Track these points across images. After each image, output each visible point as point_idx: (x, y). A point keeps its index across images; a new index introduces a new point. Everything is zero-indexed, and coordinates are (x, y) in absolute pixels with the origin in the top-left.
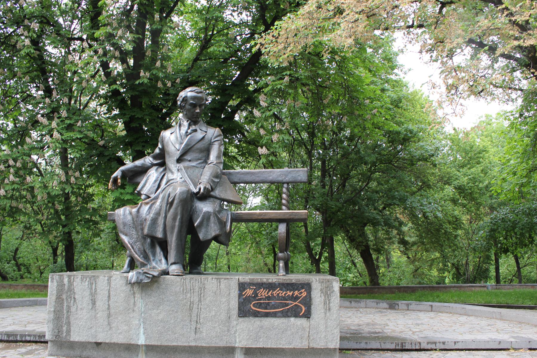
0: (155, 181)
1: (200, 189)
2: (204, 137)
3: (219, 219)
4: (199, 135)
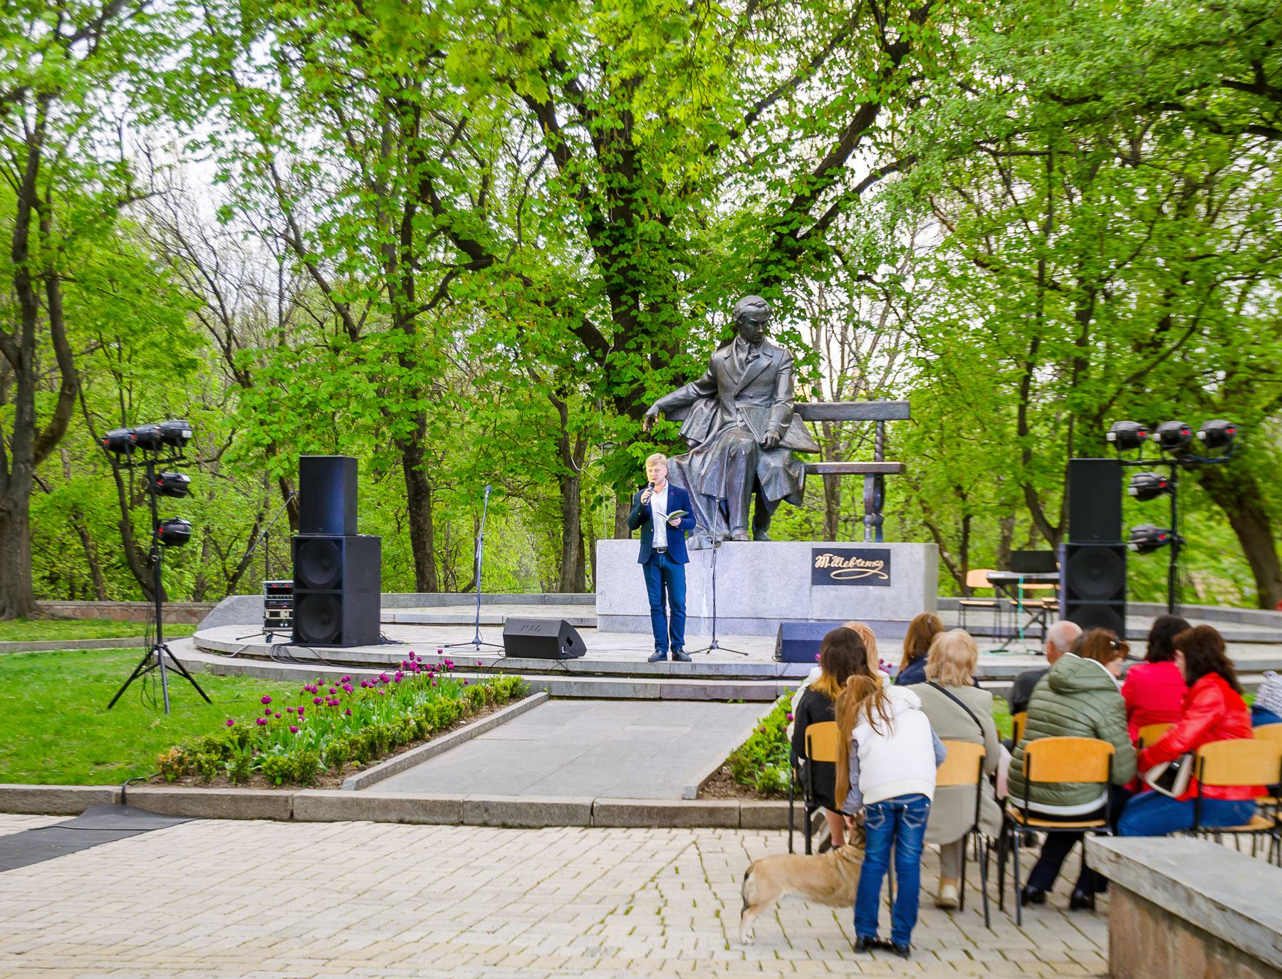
0: (705, 421)
3: (789, 475)
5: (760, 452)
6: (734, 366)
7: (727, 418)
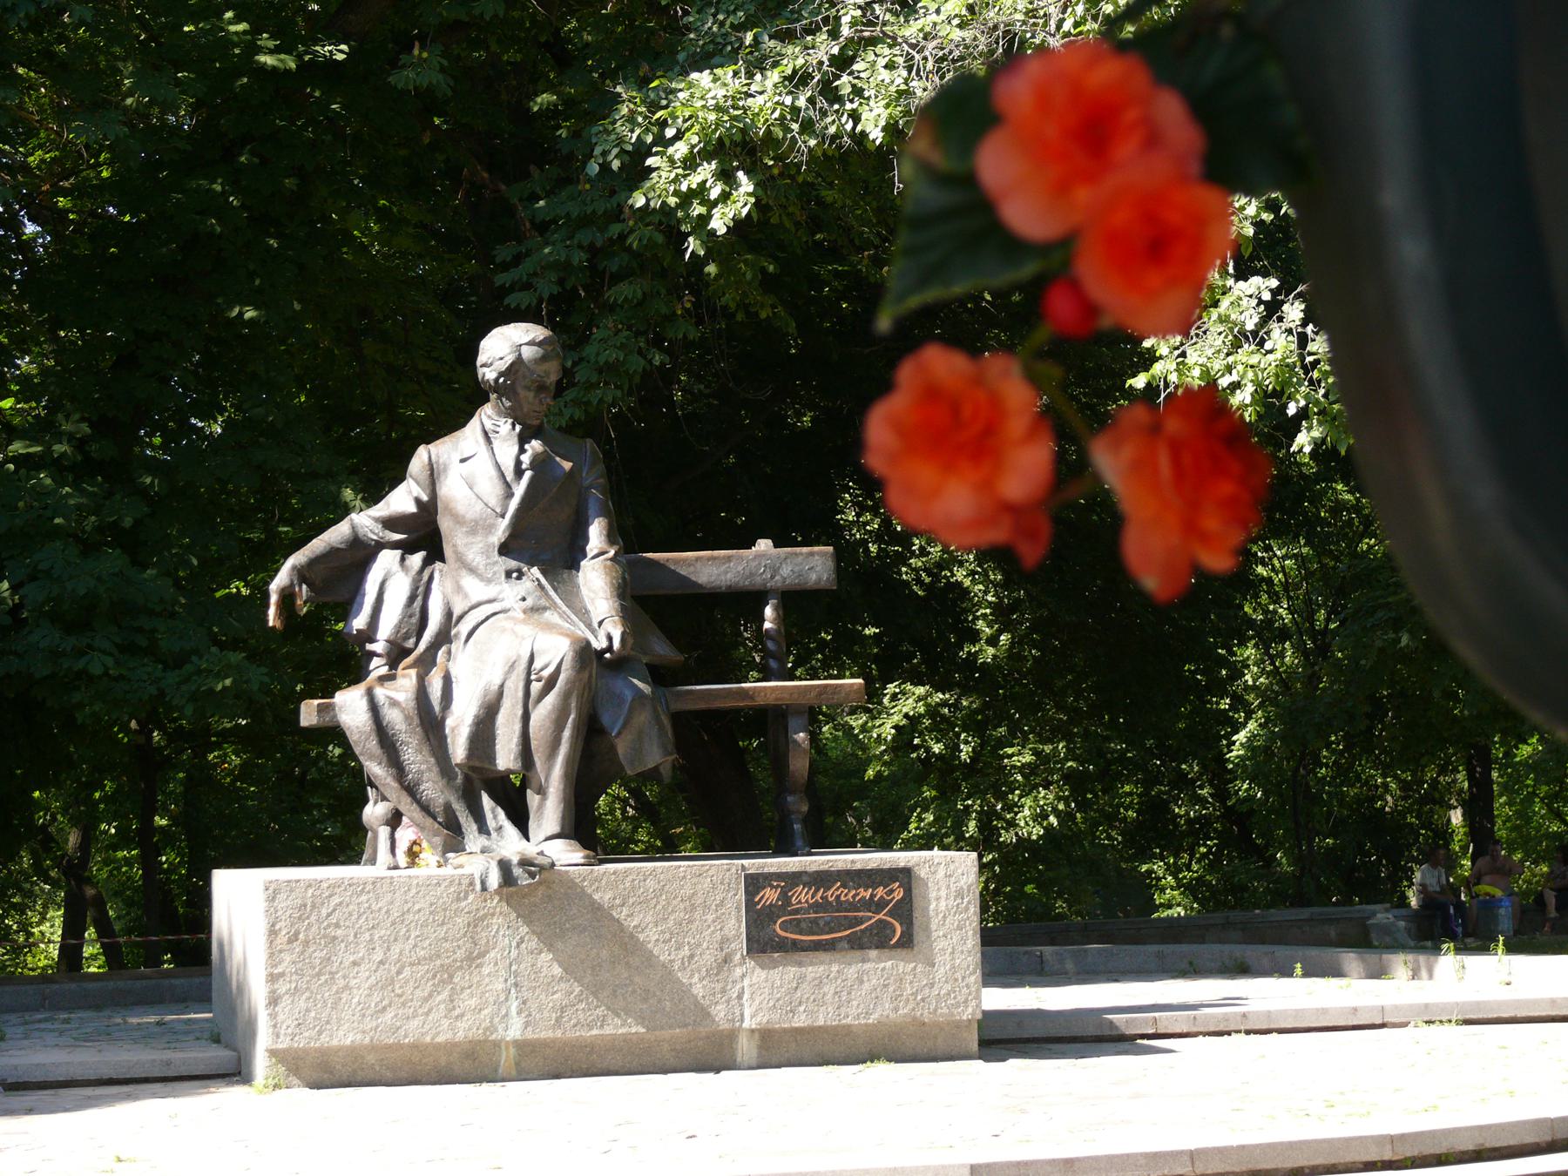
1: (610, 638)
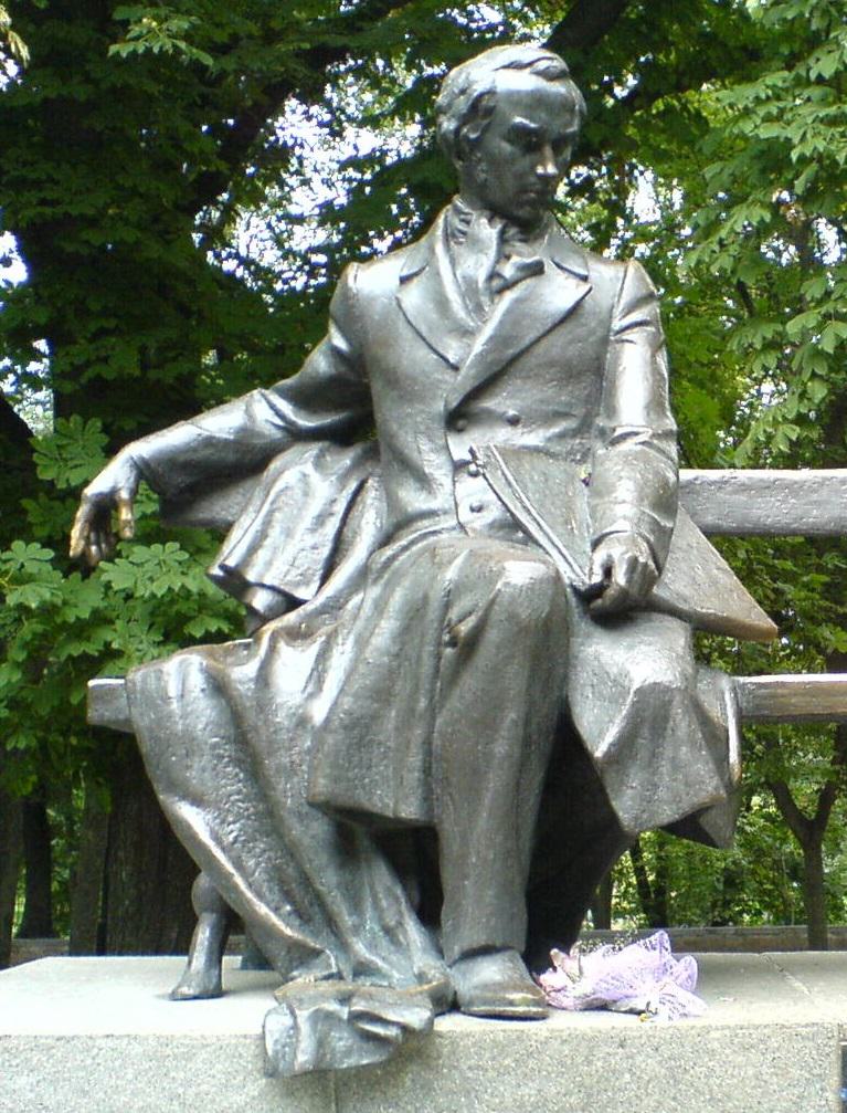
0: (321, 520)
1: (608, 572)
2: (578, 305)
4: (558, 293)
5: (583, 626)
6: (442, 304)
7: (413, 499)
